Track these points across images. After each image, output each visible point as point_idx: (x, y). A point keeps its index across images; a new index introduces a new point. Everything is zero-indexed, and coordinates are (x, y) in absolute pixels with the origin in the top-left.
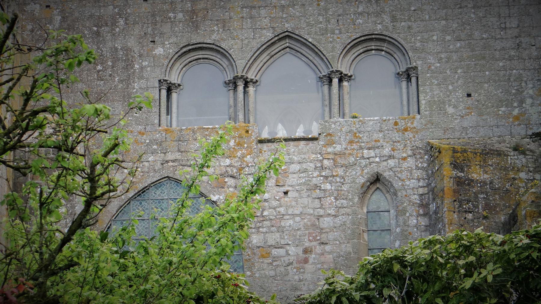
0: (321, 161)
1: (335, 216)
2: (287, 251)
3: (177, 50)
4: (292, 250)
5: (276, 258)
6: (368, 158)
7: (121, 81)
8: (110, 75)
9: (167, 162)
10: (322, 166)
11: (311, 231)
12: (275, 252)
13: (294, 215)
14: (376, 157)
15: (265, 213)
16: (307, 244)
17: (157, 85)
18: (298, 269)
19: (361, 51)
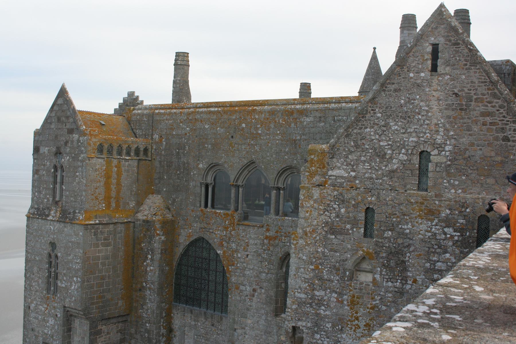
0: (263, 241)
1: (267, 274)
2: (246, 288)
3: (207, 166)
4: (248, 288)
5: (242, 291)
6: (284, 243)
7: (186, 181)
8: (182, 177)
9: (202, 228)
10: (263, 243)
11: (257, 279)
12: (242, 288)
13: (250, 269)
14: (288, 242)
15: (238, 265)
16: (254, 287)
17: (199, 185)
18: (250, 299)
19: (289, 173)
